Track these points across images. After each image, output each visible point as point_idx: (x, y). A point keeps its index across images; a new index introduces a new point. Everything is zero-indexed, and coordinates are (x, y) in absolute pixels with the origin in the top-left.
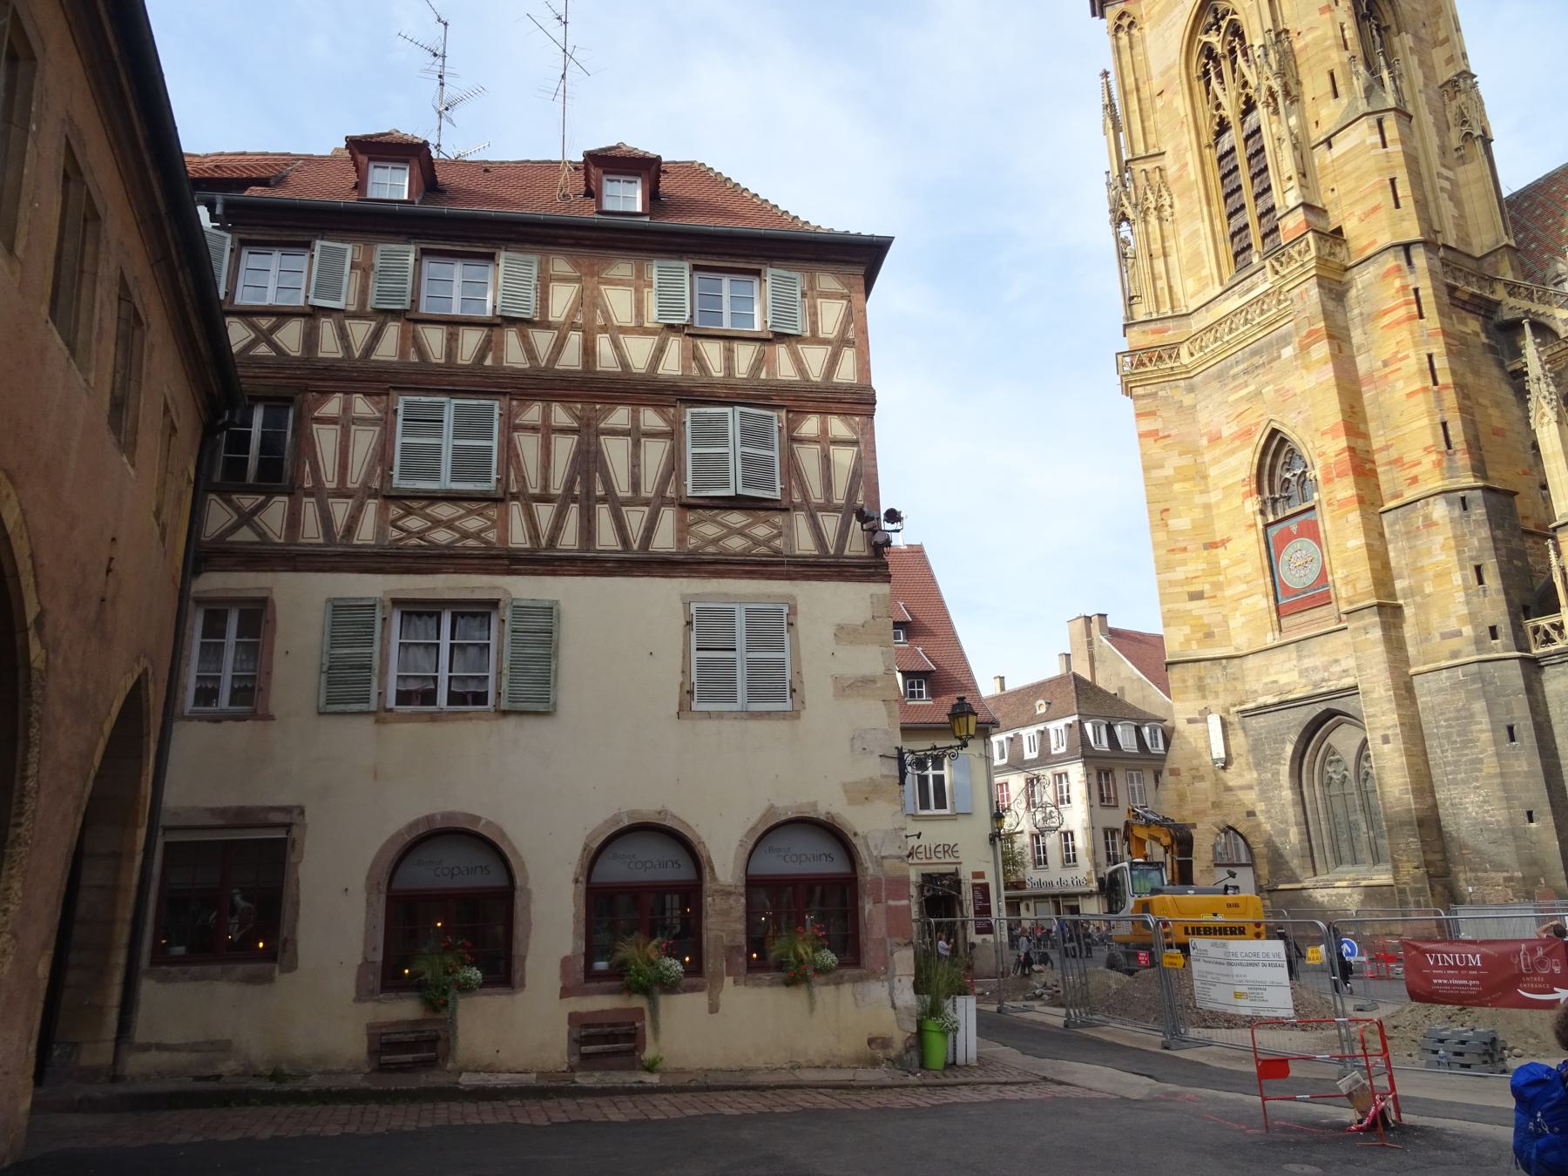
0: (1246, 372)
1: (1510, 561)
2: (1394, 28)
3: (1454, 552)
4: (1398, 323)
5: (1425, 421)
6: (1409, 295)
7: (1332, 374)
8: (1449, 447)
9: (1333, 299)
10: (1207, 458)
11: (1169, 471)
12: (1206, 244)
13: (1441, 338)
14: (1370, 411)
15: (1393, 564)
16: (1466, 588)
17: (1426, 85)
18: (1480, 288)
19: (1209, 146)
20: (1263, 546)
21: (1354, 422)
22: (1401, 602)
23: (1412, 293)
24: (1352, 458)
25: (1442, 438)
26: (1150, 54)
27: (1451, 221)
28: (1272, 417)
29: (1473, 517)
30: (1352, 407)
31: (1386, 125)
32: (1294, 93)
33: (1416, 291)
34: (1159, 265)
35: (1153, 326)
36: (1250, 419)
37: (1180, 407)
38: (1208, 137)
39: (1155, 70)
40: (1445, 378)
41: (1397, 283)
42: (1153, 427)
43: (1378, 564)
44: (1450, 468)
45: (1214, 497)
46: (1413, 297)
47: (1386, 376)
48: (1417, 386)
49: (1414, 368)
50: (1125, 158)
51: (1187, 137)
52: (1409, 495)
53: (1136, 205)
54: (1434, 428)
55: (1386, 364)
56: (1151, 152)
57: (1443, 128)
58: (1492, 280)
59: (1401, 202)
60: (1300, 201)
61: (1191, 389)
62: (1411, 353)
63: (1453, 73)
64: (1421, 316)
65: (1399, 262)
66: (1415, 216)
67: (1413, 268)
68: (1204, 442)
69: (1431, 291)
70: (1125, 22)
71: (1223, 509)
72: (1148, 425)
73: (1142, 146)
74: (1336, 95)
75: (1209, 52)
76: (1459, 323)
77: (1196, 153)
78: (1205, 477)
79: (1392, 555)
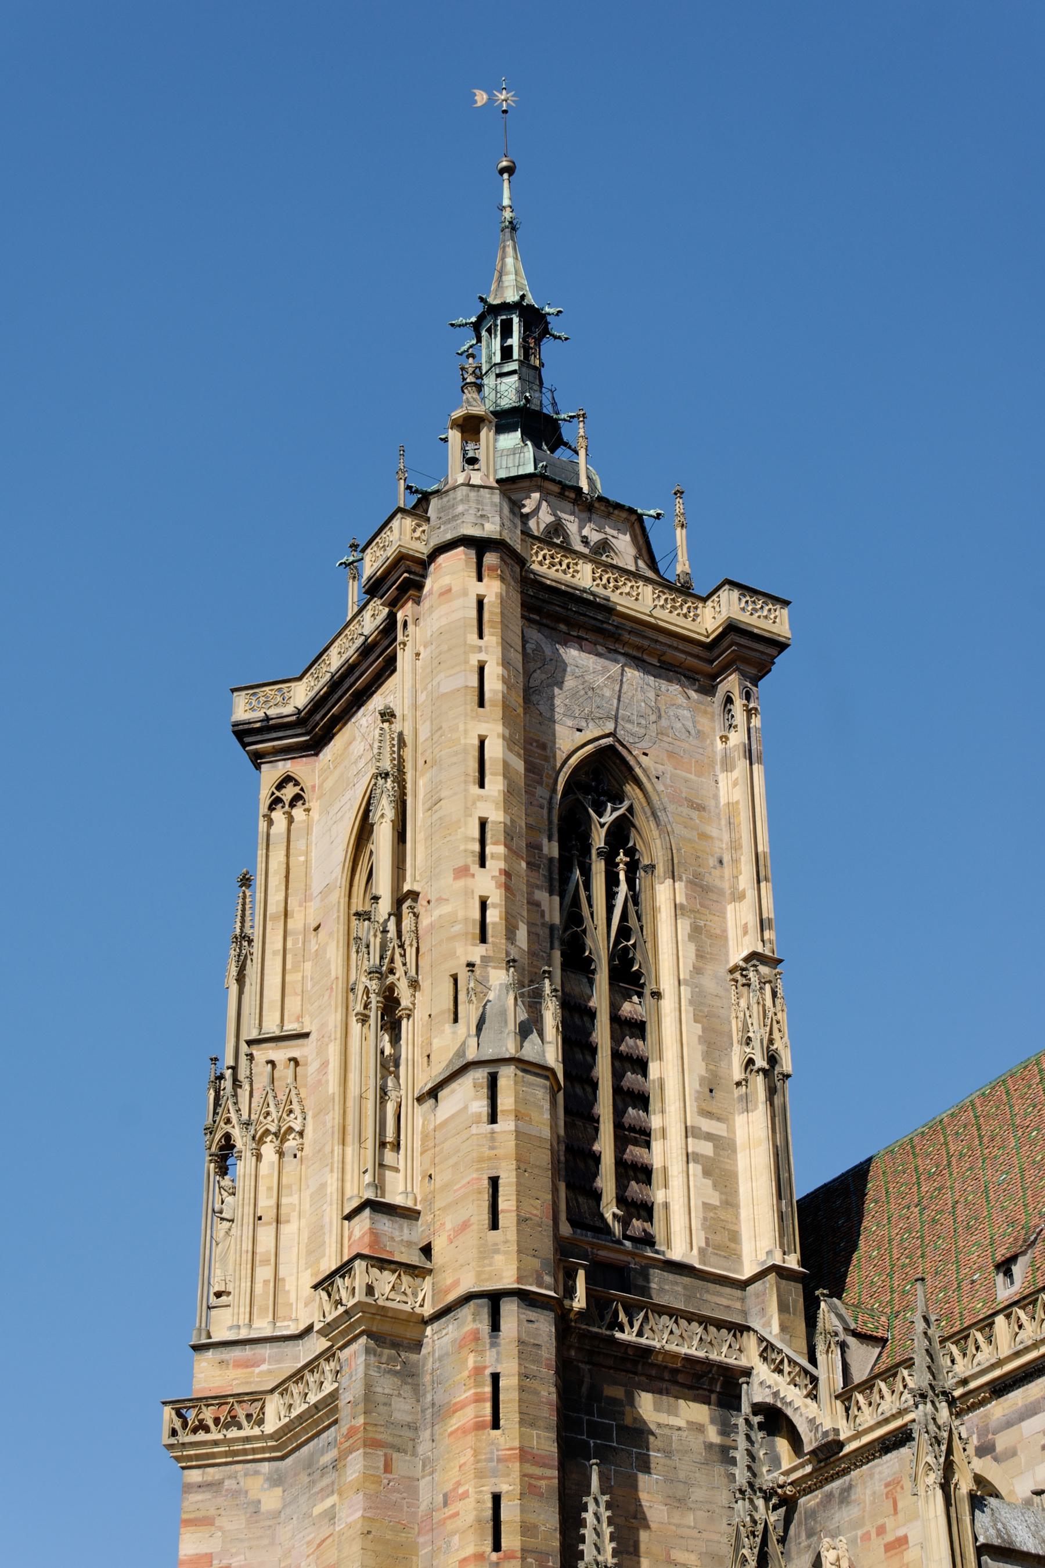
2: (660, 869)
4: (464, 1431)
6: (482, 1385)
9: (396, 1373)
17: (697, 971)
23: (488, 1381)
32: (405, 1002)
33: (495, 1378)
35: (237, 1353)
39: (316, 887)
41: (471, 1361)
46: (488, 1389)
48: (470, 1550)
51: (333, 1016)
56: (291, 1027)
62: (469, 1487)
64: (496, 1425)
65: (479, 1326)
67: (497, 1337)
74: (456, 1020)
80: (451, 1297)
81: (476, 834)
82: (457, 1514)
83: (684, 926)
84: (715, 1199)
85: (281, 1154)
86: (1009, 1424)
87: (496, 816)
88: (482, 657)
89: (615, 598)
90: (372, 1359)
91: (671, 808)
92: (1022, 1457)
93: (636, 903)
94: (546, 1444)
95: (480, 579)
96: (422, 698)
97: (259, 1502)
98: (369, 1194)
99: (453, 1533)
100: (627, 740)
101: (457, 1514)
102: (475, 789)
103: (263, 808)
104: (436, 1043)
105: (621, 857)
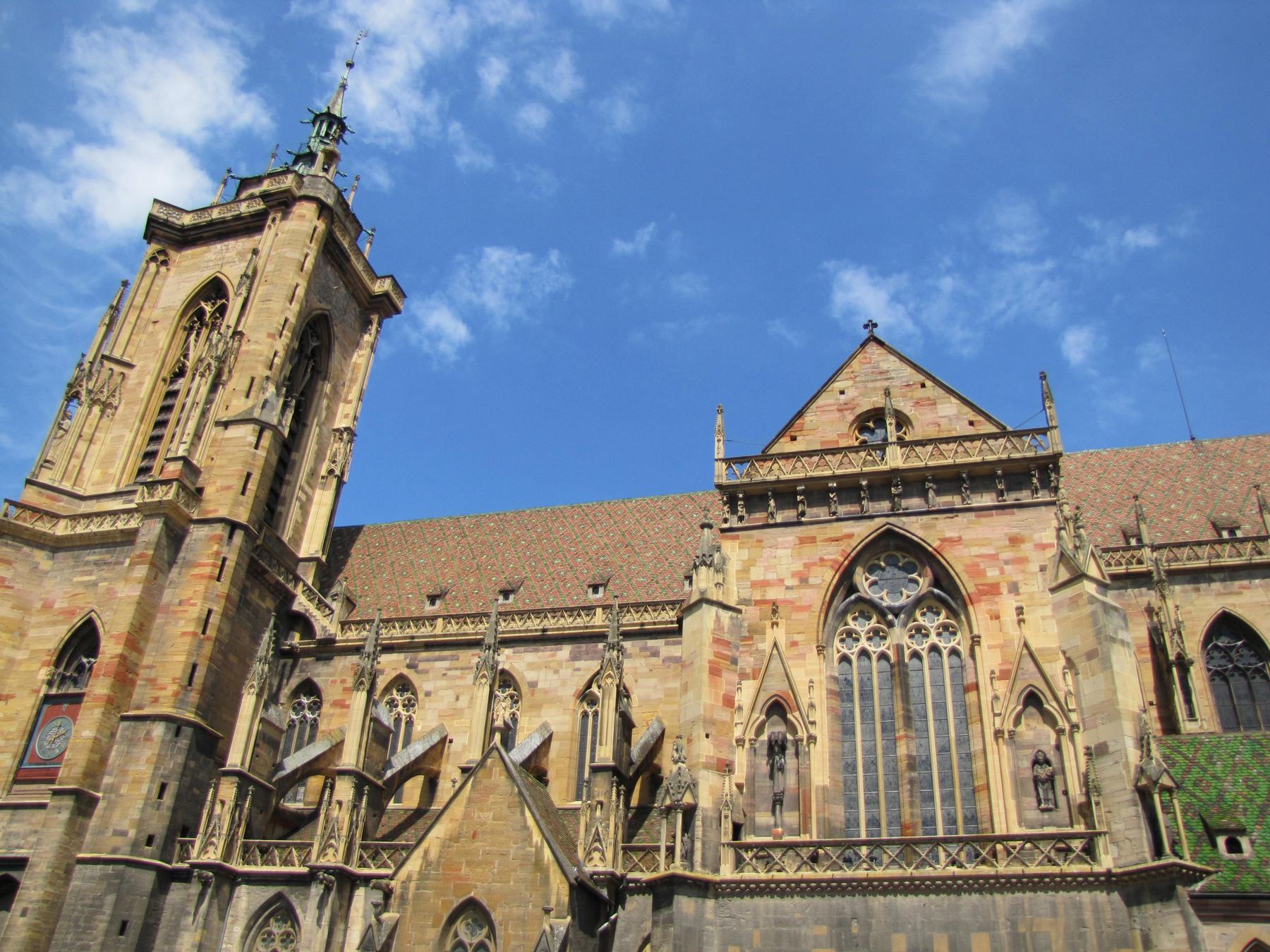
0: (96, 563)
1: (190, 788)
3: (153, 767)
4: (202, 577)
5: (182, 658)
7: (139, 593)
10: (34, 620)
12: (123, 450)
13: (223, 601)
14: (155, 634)
15: (110, 761)
16: (147, 799)
18: (287, 579)
19: (164, 380)
20: (35, 712)
21: (136, 638)
22: (100, 795)
24: (120, 664)
25: (187, 676)
26: (165, 290)
28: (95, 607)
29: (179, 744)
30: (142, 625)
33: (224, 560)
34: (82, 447)
36: (80, 602)
37: (36, 567)
38: (166, 373)
40: (211, 632)
41: (215, 548)
43: (96, 757)
45: (20, 655)
46: (220, 563)
47: (176, 612)
48: (191, 629)
49: (195, 615)
52: (147, 711)
53: (90, 392)
54: (186, 666)
55: (180, 603)
56: (126, 359)
58: (297, 579)
59: (247, 493)
60: (185, 454)
62: (199, 602)
63: (344, 425)
64: (218, 579)
66: (250, 507)
68: (38, 605)
69: (233, 564)
70: (161, 258)
71: (23, 668)
73: (121, 351)
74: (247, 396)
75: (201, 313)
76: (259, 597)
77: (153, 380)
78: (23, 635)
79: (113, 753)
80: (211, 516)
82: (186, 611)
86: (428, 660)
87: (292, 320)
88: (309, 251)
92: (431, 675)
96: (273, 253)
99: (182, 619)
100: (333, 317)
101: (186, 611)
102: (288, 304)
103: (147, 258)
104: (234, 402)
105: (312, 363)
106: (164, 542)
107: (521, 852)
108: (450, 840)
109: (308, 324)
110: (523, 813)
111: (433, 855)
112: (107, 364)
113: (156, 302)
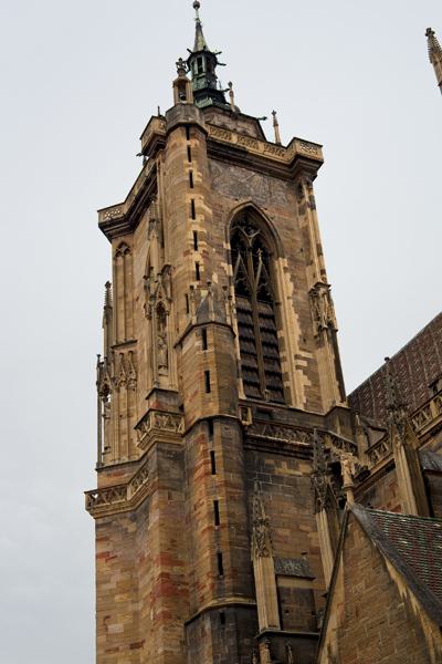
2: (276, 254)
4: (201, 477)
5: (207, 554)
8: (221, 573)
10: (139, 573)
11: (112, 586)
17: (294, 293)
27: (303, 389)
29: (227, 629)
30: (173, 541)
31: (208, 332)
33: (212, 453)
35: (115, 471)
39: (136, 283)
42: (105, 550)
44: (219, 590)
45: (140, 606)
46: (209, 458)
48: (206, 526)
50: (114, 344)
53: (114, 379)
54: (212, 559)
57: (304, 323)
61: (134, 519)
62: (204, 500)
64: (214, 473)
68: (138, 561)
69: (221, 454)
70: (124, 248)
72: (105, 548)
76: (289, 468)
78: (136, 590)
81: (193, 237)
83: (288, 275)
84: (309, 384)
85: (127, 389)
89: (249, 148)
90: (161, 454)
91: (278, 230)
93: (267, 269)
94: (234, 478)
95: (188, 139)
97: (127, 529)
98: (155, 386)
100: (258, 204)
102: (191, 220)
104: (181, 323)
106: (166, 464)
107: (395, 612)
108: (342, 627)
109: (233, 225)
110: (385, 567)
111: (334, 649)
112: (117, 352)
113: (133, 284)
